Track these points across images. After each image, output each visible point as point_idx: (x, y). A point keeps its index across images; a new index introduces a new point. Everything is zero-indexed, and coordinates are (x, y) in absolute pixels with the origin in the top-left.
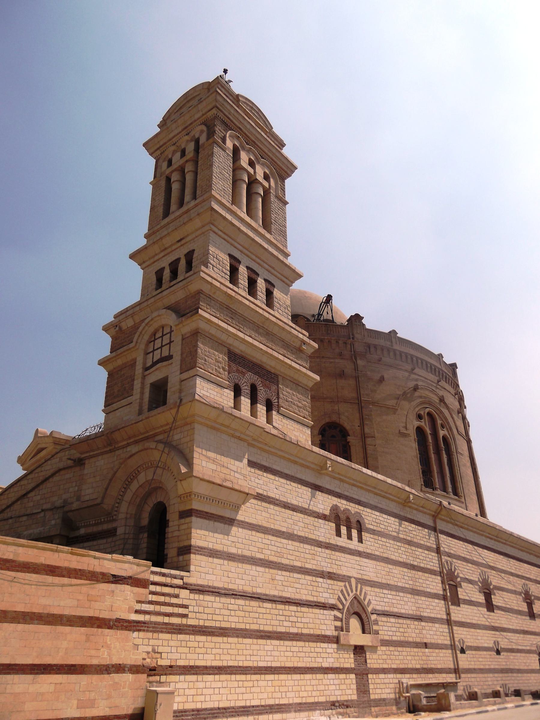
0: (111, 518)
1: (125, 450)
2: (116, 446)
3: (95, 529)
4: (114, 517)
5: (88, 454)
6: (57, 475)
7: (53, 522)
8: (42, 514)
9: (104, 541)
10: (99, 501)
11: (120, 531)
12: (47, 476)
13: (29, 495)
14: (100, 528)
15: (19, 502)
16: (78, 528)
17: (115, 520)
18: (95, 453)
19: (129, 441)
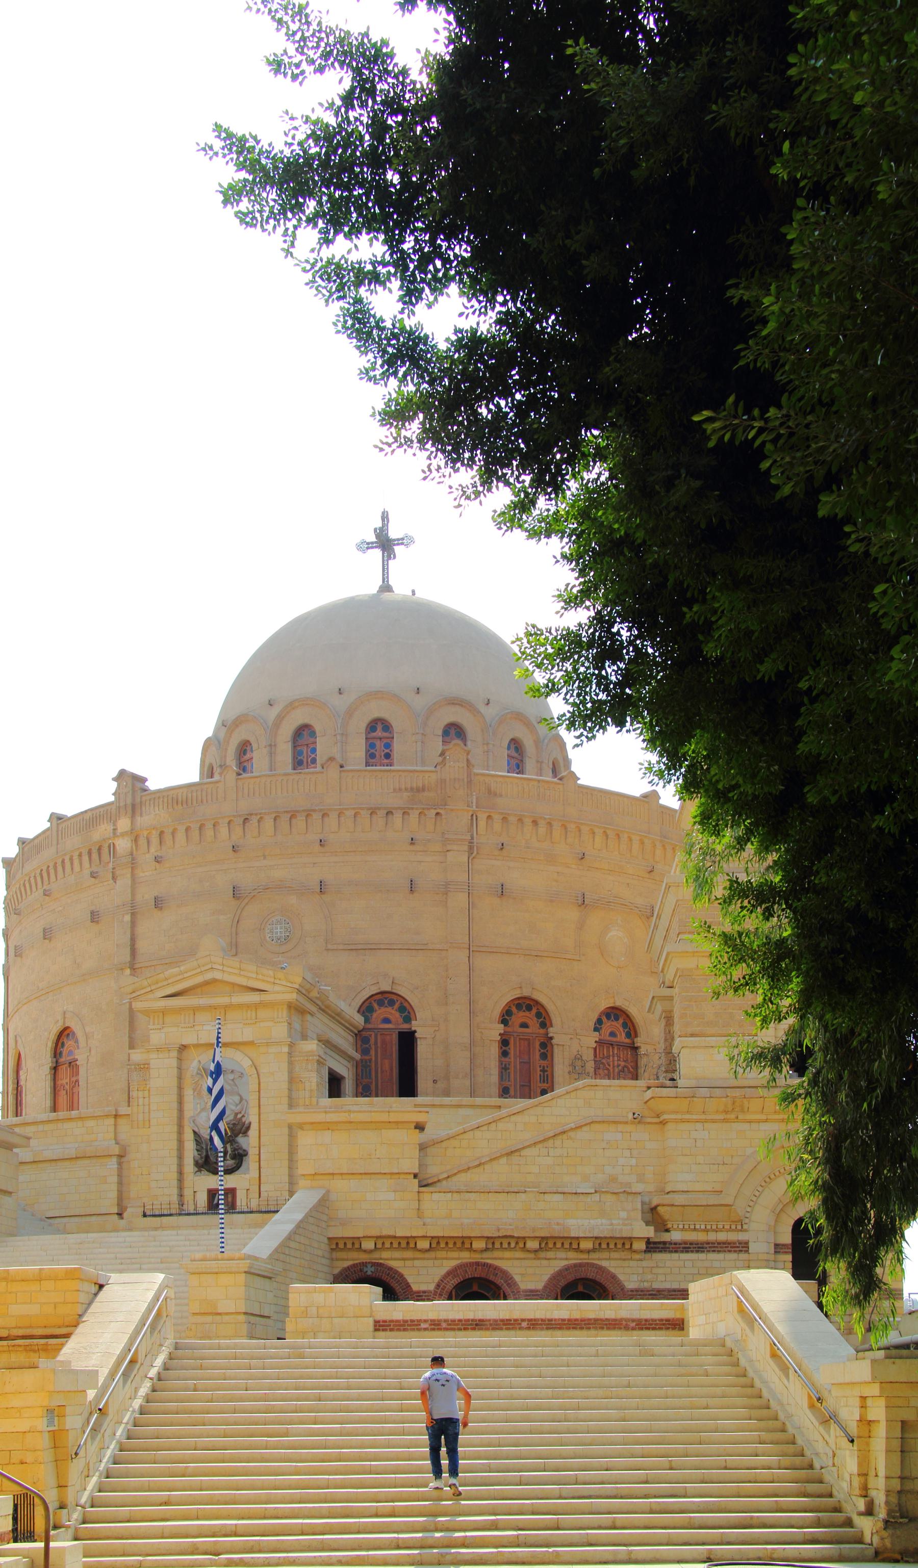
0: (739, 1227)
1: (754, 1125)
2: (740, 1117)
3: (701, 1237)
4: (745, 1227)
5: (679, 1116)
6: (584, 1129)
7: (623, 1214)
8: (596, 1197)
9: (721, 1256)
10: (729, 1201)
11: (752, 1247)
12: (567, 1128)
13: (523, 1153)
14: (712, 1237)
15: (504, 1160)
16: (667, 1231)
17: (746, 1231)
18: (694, 1117)
19: (769, 1117)
